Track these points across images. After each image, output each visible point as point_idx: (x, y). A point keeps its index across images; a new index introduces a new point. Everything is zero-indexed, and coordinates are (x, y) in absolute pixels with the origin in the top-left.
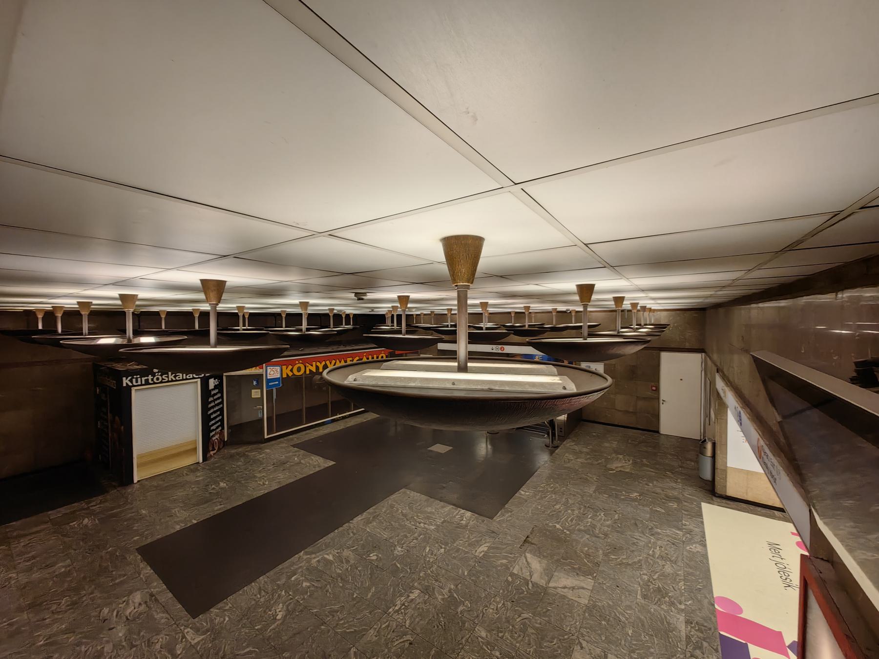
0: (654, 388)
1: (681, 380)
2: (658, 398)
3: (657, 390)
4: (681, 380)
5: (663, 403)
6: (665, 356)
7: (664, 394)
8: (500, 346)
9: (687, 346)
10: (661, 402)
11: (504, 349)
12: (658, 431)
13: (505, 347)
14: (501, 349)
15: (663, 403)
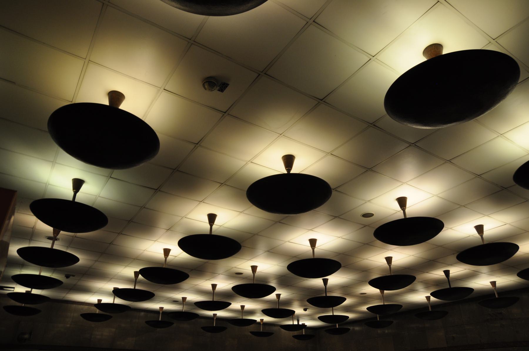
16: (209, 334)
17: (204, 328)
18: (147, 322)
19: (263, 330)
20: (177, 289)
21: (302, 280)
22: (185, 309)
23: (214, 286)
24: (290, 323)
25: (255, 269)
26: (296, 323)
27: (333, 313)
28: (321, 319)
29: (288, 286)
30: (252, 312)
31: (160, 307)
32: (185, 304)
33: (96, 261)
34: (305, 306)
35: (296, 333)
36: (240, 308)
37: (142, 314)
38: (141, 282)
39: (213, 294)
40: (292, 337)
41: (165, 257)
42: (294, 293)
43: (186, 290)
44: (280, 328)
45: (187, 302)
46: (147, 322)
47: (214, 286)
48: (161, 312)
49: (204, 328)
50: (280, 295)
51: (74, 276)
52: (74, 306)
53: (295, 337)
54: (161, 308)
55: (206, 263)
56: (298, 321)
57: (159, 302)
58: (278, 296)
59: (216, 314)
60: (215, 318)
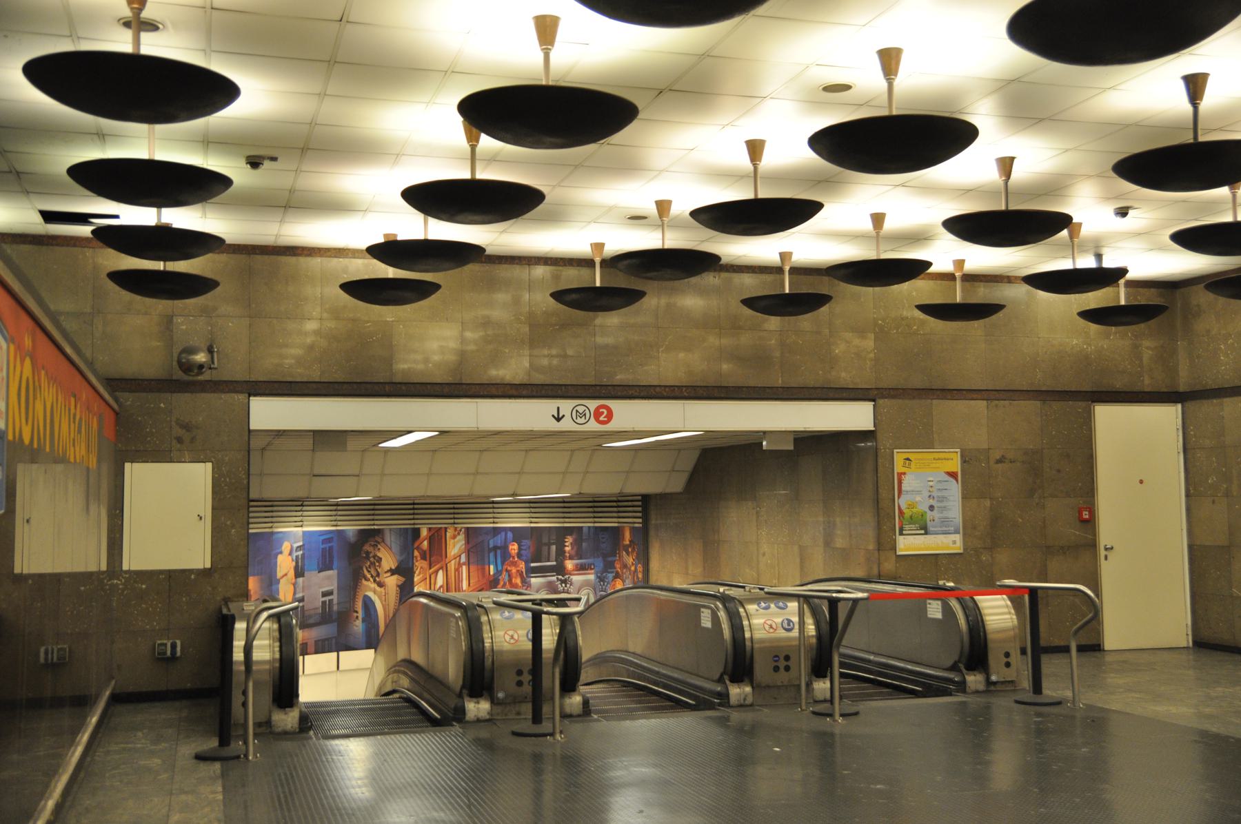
0: (1086, 515)
1: (1141, 482)
2: (1092, 545)
3: (1089, 523)
4: (1141, 482)
5: (1106, 558)
6: (1105, 415)
7: (1107, 532)
8: (593, 404)
9: (1147, 384)
10: (1103, 553)
11: (610, 416)
12: (1099, 645)
13: (615, 405)
14: (597, 414)
15: (1106, 558)
16: (774, 322)
17: (750, 303)
18: (558, 296)
19: (963, 297)
20: (628, 167)
21: (1097, 91)
22: (674, 240)
23: (755, 148)
24: (1065, 264)
25: (893, 62)
26: (1086, 262)
27: (1235, 215)
28: (1189, 239)
29: (1041, 120)
30: (918, 237)
31: (591, 244)
32: (668, 226)
33: (322, 95)
34: (1117, 197)
35: (1094, 299)
36: (868, 226)
37: (540, 271)
38: (493, 159)
39: (752, 180)
40: (1078, 317)
41: (543, 49)
42: (1067, 150)
43: (661, 171)
44: (1025, 288)
45: (676, 217)
46: (558, 296)
47: (755, 148)
48: (598, 260)
49: (750, 303)
50: (1012, 159)
51: (274, 159)
52: (317, 261)
53: (1091, 315)
54: (599, 247)
55: (705, 55)
56: (1099, 257)
57: (584, 224)
58: (1006, 165)
59: (790, 254)
60: (787, 268)
